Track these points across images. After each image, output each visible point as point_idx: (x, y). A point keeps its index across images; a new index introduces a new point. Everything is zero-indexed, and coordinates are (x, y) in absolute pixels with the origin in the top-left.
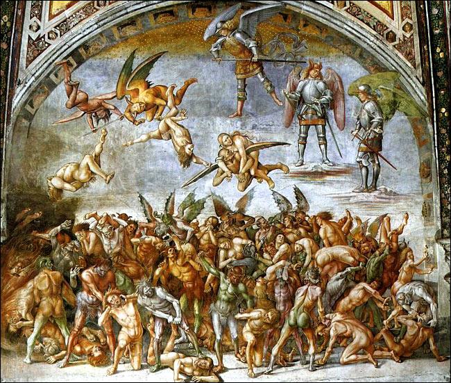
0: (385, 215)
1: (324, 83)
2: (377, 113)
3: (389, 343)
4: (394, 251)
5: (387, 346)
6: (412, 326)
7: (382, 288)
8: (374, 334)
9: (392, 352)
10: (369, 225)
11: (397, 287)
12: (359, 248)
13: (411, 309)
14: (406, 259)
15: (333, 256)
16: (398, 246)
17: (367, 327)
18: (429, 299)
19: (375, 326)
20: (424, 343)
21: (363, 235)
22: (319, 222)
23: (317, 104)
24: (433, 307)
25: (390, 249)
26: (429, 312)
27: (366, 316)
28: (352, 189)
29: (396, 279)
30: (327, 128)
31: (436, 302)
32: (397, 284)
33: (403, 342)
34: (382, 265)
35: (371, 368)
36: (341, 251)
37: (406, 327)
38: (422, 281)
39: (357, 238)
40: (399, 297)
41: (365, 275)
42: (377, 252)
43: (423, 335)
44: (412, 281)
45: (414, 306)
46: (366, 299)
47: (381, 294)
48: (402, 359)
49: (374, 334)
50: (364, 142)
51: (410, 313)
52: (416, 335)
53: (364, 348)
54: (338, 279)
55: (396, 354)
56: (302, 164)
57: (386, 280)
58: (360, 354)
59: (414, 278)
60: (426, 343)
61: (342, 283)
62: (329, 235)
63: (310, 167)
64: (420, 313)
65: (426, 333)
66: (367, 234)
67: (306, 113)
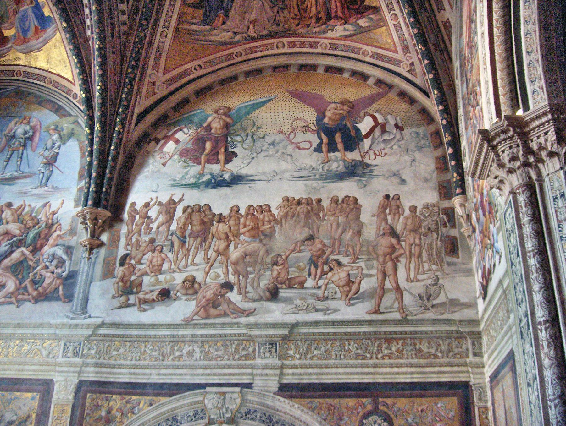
0: (48, 202)
1: (30, 126)
2: (59, 140)
3: (30, 289)
4: (49, 226)
5: (27, 292)
6: (49, 277)
7: (36, 250)
8: (20, 284)
9: (30, 296)
10: (36, 209)
11: (45, 250)
12: (25, 225)
13: (51, 265)
14: (55, 231)
15: (7, 231)
16: (53, 222)
17: (17, 278)
18: (65, 257)
19: (23, 277)
20: (56, 289)
21: (31, 215)
22: (4, 208)
23: (22, 138)
24: (67, 263)
25: (46, 224)
26: (64, 267)
27: (18, 271)
28: (30, 187)
29: (46, 245)
30: (25, 151)
31: (71, 259)
32: (46, 248)
33: (40, 289)
34: (38, 236)
35: (13, 307)
36: (14, 228)
37: (45, 278)
38: (64, 245)
39: (27, 218)
40: (46, 256)
41: (25, 243)
42: (37, 227)
43: (55, 285)
44: (57, 245)
45: (55, 262)
46: (21, 259)
47: (33, 255)
48: (36, 302)
49: (20, 284)
50: (46, 158)
51: (50, 268)
52: (50, 284)
53: (12, 293)
54: (6, 246)
55: (33, 298)
56: (3, 174)
57: (38, 245)
58: (8, 298)
59: (59, 243)
60: (57, 289)
61: (9, 249)
62: (8, 216)
63: (8, 175)
64: (57, 267)
65: (58, 282)
66: (34, 214)
67: (14, 144)
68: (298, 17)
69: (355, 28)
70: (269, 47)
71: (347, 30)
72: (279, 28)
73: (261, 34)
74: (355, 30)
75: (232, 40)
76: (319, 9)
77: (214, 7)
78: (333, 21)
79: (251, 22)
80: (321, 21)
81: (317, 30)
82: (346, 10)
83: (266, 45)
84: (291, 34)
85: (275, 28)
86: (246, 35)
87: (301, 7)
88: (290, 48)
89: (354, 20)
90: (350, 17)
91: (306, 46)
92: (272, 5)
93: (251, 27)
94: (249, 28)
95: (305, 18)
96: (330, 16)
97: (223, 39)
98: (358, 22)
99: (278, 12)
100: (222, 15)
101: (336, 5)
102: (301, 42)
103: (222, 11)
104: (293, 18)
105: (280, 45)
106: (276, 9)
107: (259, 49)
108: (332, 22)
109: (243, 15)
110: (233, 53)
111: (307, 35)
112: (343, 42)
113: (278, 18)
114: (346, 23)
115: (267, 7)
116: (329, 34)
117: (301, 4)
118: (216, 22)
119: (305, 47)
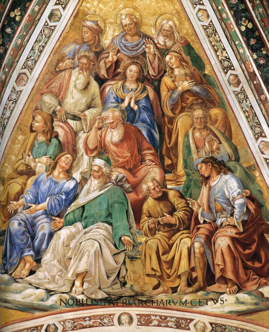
68: (158, 274)
69: (255, 301)
70: (106, 321)
71: (243, 303)
72: (124, 289)
73: (93, 296)
74: (256, 304)
75: (41, 303)
76: (193, 265)
77: (19, 245)
78: (217, 285)
79: (78, 275)
80: (196, 285)
81: (188, 298)
82: (241, 270)
83: (101, 317)
84: (146, 302)
85: (117, 289)
86: (67, 296)
87: (163, 258)
88: (142, 325)
89: (255, 287)
90: (248, 280)
91: (170, 324)
92: (117, 251)
93: (78, 283)
94: (73, 285)
95: (169, 277)
96: (213, 276)
97: (28, 300)
98: (261, 290)
99: (124, 262)
100: (31, 259)
101: (224, 260)
102: (161, 317)
103: (32, 253)
104: (148, 275)
105: (124, 318)
106: (121, 257)
107: (87, 323)
108: (214, 288)
109: (65, 263)
110: (42, 326)
111: (173, 306)
112: (235, 323)
113: (123, 272)
114: (239, 290)
115: (107, 253)
116: (210, 307)
117: (164, 254)
118: (19, 269)
119: (167, 326)
